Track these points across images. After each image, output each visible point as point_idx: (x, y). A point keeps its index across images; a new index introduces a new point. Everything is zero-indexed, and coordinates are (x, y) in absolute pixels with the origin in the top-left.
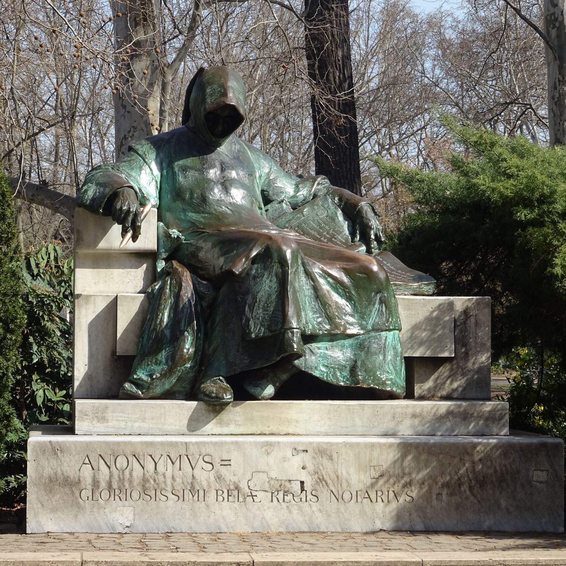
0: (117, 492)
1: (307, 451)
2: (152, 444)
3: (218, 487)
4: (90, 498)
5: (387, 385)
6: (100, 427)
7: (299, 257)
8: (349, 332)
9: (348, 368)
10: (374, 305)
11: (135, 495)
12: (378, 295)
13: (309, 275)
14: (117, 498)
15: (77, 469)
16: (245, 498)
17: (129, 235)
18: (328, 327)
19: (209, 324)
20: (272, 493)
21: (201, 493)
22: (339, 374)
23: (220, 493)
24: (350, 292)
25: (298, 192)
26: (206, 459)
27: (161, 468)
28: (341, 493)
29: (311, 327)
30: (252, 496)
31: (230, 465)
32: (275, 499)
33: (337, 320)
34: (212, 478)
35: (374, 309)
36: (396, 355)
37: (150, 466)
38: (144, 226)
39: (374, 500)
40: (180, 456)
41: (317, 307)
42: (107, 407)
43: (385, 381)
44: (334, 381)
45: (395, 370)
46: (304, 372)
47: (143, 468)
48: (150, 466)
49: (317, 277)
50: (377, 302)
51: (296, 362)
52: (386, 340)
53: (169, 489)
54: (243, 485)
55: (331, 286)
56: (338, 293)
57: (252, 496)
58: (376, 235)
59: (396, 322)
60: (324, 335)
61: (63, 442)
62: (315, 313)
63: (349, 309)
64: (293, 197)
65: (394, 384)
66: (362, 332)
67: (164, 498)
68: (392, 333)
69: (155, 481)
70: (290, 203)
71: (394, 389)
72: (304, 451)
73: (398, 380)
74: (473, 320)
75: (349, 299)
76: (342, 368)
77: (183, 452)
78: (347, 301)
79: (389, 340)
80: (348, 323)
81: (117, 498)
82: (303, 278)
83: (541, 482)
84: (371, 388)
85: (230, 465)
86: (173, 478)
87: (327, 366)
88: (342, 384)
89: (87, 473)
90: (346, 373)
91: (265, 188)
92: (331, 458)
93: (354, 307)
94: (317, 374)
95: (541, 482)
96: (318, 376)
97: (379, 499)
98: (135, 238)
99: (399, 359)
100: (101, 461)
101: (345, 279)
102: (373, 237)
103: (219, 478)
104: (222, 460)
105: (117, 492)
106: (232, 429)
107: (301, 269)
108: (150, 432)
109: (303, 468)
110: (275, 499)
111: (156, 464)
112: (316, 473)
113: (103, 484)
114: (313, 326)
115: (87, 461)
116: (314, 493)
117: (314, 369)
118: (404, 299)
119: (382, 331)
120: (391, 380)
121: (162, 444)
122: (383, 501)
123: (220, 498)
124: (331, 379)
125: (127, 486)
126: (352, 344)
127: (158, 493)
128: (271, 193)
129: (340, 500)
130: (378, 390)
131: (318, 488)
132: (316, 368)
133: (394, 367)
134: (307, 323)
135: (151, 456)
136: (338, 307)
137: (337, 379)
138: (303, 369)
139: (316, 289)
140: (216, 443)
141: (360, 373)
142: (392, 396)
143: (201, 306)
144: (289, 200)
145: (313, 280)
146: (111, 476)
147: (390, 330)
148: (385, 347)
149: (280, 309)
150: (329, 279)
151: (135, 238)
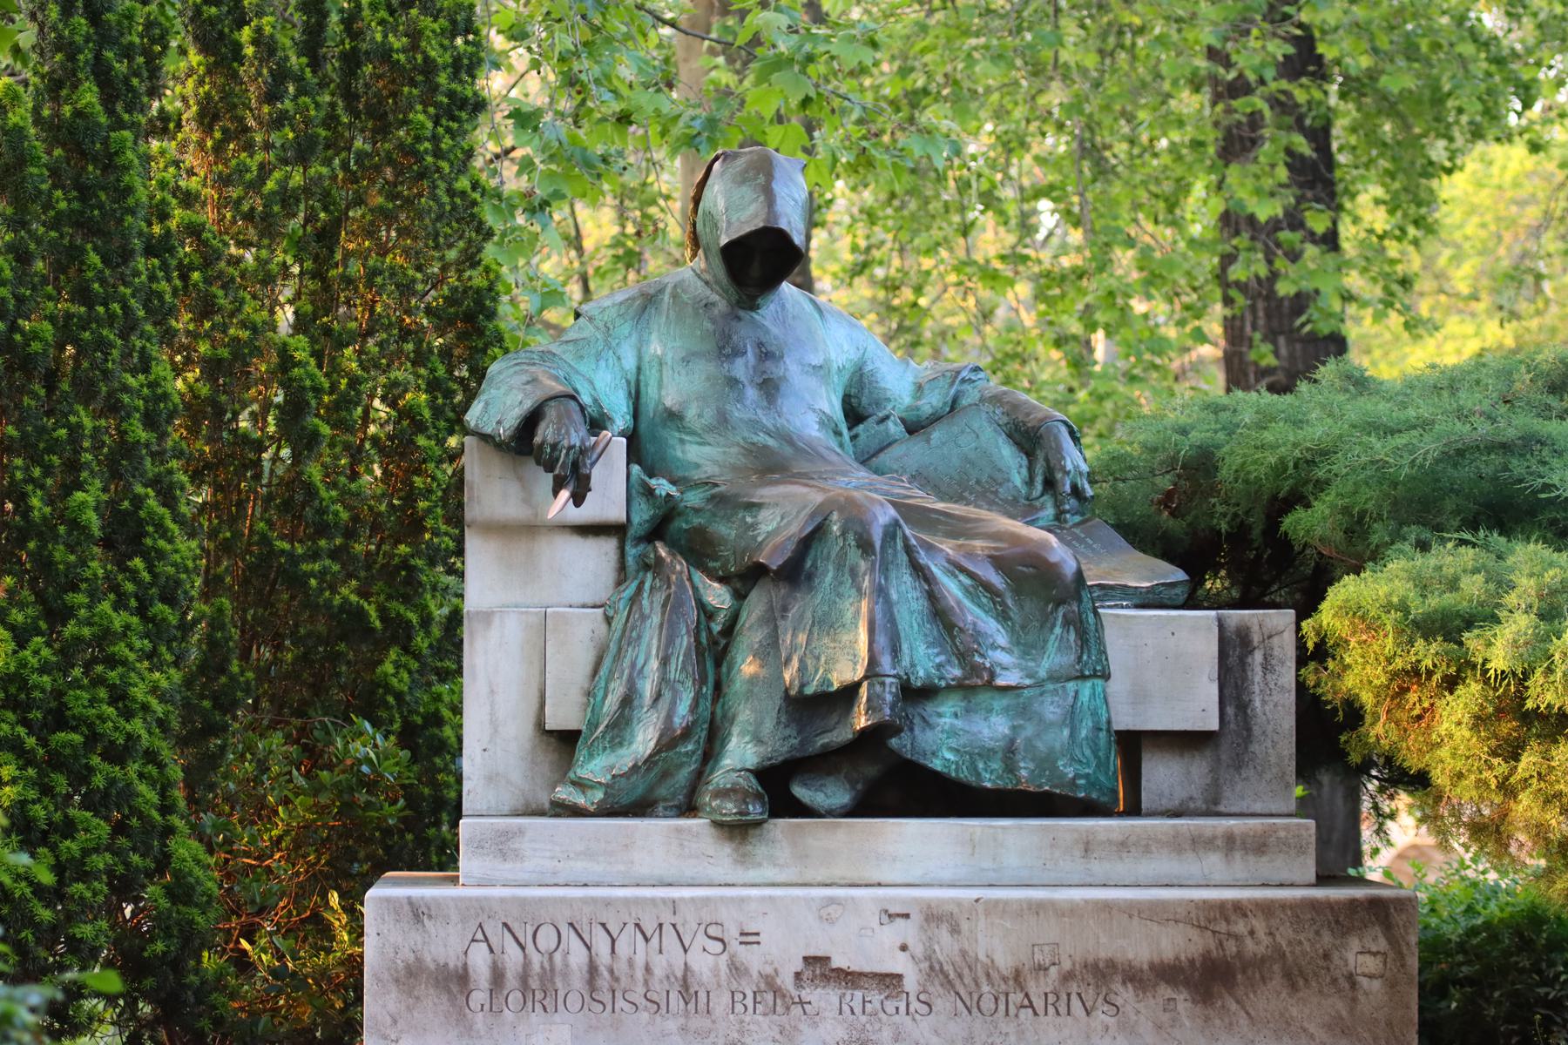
0: (539, 995)
1: (907, 916)
2: (608, 903)
3: (734, 986)
4: (487, 1007)
6: (506, 869)
7: (899, 533)
8: (1000, 682)
9: (1000, 755)
10: (1053, 626)
11: (574, 1001)
13: (919, 571)
14: (538, 1005)
15: (460, 950)
16: (788, 1008)
17: (565, 494)
19: (724, 669)
22: (981, 766)
23: (739, 997)
24: (1003, 604)
25: (919, 399)
26: (712, 931)
27: (623, 947)
28: (975, 997)
29: (921, 673)
33: (977, 658)
34: (724, 968)
37: (601, 944)
38: (597, 474)
39: (1041, 1011)
40: (661, 925)
42: (521, 832)
43: (1074, 779)
44: (972, 779)
45: (1096, 757)
47: (589, 948)
48: (601, 944)
50: (1059, 622)
51: (894, 742)
53: (641, 990)
55: (966, 590)
56: (980, 606)
58: (1075, 488)
59: (1099, 661)
60: (949, 687)
61: (434, 899)
63: (1002, 639)
64: (909, 408)
65: (1092, 784)
66: (1028, 682)
67: (627, 1007)
68: (1089, 684)
69: (611, 972)
70: (903, 420)
71: (1094, 796)
73: (1102, 778)
74: (1258, 657)
75: (1003, 617)
76: (987, 754)
77: (667, 918)
81: (538, 1005)
82: (907, 578)
83: (1371, 977)
86: (648, 969)
87: (958, 751)
88: (988, 785)
89: (479, 960)
90: (996, 765)
91: (853, 391)
92: (955, 930)
93: (1012, 631)
94: (937, 765)
95: (1371, 977)
96: (939, 769)
97: (1051, 1010)
98: (578, 499)
99: (1103, 735)
100: (507, 935)
101: (997, 580)
102: (1068, 488)
103: (737, 969)
105: (539, 995)
106: (769, 873)
107: (903, 558)
108: (608, 880)
109: (904, 948)
111: (613, 941)
112: (928, 958)
113: (511, 980)
115: (479, 936)
116: (922, 997)
118: (1118, 616)
119: (1069, 679)
120: (1087, 776)
121: (626, 901)
122: (1058, 1013)
123: (739, 1008)
124: (965, 775)
125: (559, 985)
127: (618, 995)
128: (864, 401)
129: (975, 1010)
130: (1060, 796)
131: (931, 989)
132: (933, 754)
134: (913, 665)
135: (603, 925)
136: (978, 634)
137: (978, 774)
140: (732, 899)
143: (709, 630)
144: (904, 415)
145: (927, 580)
146: (527, 964)
147: (1083, 677)
150: (962, 577)
151: (578, 499)
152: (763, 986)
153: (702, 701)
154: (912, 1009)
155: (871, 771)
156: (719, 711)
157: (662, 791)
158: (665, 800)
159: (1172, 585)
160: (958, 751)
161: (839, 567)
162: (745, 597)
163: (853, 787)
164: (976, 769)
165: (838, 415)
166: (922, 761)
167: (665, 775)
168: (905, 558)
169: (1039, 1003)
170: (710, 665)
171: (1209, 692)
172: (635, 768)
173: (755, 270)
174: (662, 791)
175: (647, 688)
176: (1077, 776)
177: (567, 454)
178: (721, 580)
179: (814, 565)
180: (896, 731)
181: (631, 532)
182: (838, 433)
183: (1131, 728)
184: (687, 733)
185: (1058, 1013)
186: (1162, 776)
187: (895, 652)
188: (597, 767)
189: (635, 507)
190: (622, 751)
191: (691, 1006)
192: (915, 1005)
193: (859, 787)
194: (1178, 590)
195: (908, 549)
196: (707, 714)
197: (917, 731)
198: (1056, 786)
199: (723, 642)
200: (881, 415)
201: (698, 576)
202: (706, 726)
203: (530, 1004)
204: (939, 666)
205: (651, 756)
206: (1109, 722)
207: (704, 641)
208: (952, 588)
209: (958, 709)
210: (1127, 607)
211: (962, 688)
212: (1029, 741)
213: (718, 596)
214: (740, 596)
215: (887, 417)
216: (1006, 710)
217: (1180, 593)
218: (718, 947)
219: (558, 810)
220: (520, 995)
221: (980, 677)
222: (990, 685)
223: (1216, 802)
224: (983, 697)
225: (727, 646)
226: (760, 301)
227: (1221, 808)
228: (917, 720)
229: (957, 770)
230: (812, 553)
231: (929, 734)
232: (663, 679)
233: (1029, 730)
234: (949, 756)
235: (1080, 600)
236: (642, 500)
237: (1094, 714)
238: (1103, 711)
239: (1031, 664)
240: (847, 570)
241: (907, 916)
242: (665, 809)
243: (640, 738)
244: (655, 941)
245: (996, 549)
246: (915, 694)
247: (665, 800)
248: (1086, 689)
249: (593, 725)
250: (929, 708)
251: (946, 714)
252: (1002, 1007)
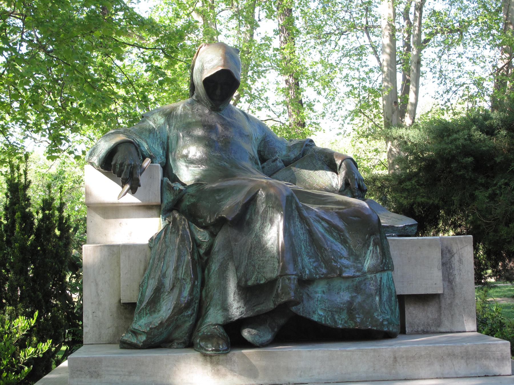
5: (384, 325)
8: (345, 275)
9: (346, 311)
10: (369, 246)
12: (372, 237)
18: (324, 271)
19: (206, 272)
22: (336, 317)
29: (307, 272)
35: (369, 251)
36: (390, 296)
41: (313, 251)
43: (382, 322)
45: (391, 310)
46: (302, 317)
49: (312, 221)
51: (294, 309)
52: (381, 281)
55: (326, 229)
62: (310, 257)
65: (389, 323)
66: (358, 274)
70: (283, 161)
71: (391, 329)
73: (393, 320)
74: (456, 257)
75: (344, 242)
76: (340, 310)
78: (342, 244)
79: (384, 281)
80: (347, 267)
82: (298, 223)
84: (370, 329)
87: (325, 310)
88: (340, 326)
90: (344, 316)
91: (262, 149)
94: (315, 318)
96: (316, 320)
99: (393, 298)
107: (296, 213)
114: (310, 271)
118: (394, 240)
119: (377, 272)
120: (387, 320)
124: (329, 322)
126: (349, 286)
133: (389, 307)
134: (303, 268)
137: (336, 322)
138: (301, 314)
139: (311, 233)
141: (357, 316)
142: (388, 336)
143: (199, 252)
144: (283, 159)
147: (383, 270)
148: (380, 288)
150: (323, 223)
153: (195, 289)
155: (282, 321)
156: (204, 293)
157: (176, 335)
158: (177, 339)
159: (411, 226)
160: (325, 310)
162: (216, 235)
163: (273, 330)
164: (334, 319)
165: (257, 156)
166: (308, 317)
167: (177, 327)
168: (297, 213)
170: (199, 270)
171: (437, 274)
172: (161, 324)
173: (218, 92)
174: (176, 335)
175: (168, 283)
176: (384, 320)
177: (127, 168)
178: (205, 228)
179: (251, 218)
180: (297, 303)
181: (163, 207)
182: (257, 163)
183: (402, 293)
184: (188, 305)
186: (414, 314)
187: (295, 262)
188: (143, 323)
189: (165, 196)
190: (155, 315)
193: (276, 330)
194: (413, 228)
195: (298, 208)
196: (198, 295)
197: (305, 302)
198: (374, 326)
199: (206, 258)
200: (274, 158)
201: (193, 226)
202: (197, 301)
204: (315, 268)
205: (169, 318)
206: (395, 292)
207: (196, 257)
208: (319, 229)
209: (324, 289)
210: (395, 236)
211: (326, 278)
212: (360, 304)
213: (202, 236)
214: (213, 235)
215: (276, 159)
216: (348, 288)
217: (414, 229)
219: (125, 346)
221: (335, 272)
222: (340, 276)
223: (439, 326)
224: (337, 283)
225: (207, 262)
226: (221, 107)
227: (442, 330)
228: (305, 296)
229: (325, 320)
230: (249, 211)
231: (311, 302)
232: (176, 279)
233: (360, 299)
234: (321, 313)
235: (380, 233)
236: (168, 192)
237: (389, 288)
238: (392, 287)
239: (360, 265)
242: (178, 344)
243: (164, 308)
245: (339, 209)
246: (304, 283)
247: (177, 339)
248: (385, 275)
249: (141, 302)
250: (311, 288)
251: (319, 290)
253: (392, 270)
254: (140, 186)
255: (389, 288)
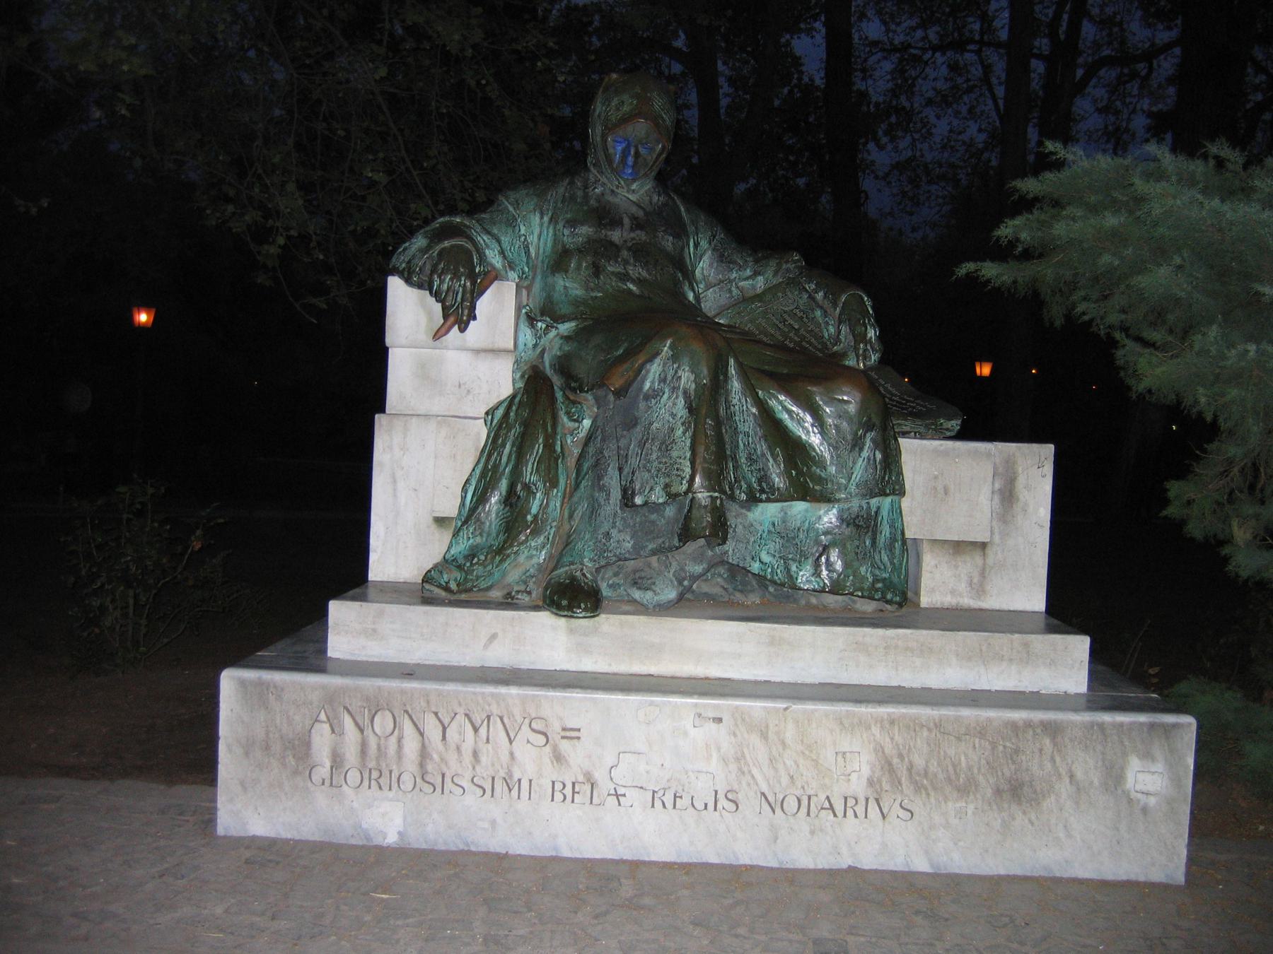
0: (375, 774)
4: (327, 782)
10: (861, 449)
14: (373, 783)
20: (654, 792)
21: (525, 784)
23: (558, 786)
30: (617, 795)
31: (578, 738)
32: (658, 804)
36: (893, 539)
37: (433, 731)
39: (840, 813)
40: (489, 717)
47: (422, 734)
48: (433, 731)
54: (600, 775)
57: (617, 795)
68: (889, 499)
72: (714, 719)
77: (495, 710)
79: (885, 512)
85: (578, 738)
97: (850, 813)
104: (564, 729)
105: (375, 774)
110: (658, 804)
111: (444, 729)
116: (730, 796)
117: (748, 559)
122: (856, 816)
123: (559, 796)
129: (778, 810)
135: (436, 714)
147: (883, 494)
149: (688, 455)
152: (581, 778)
154: (719, 806)
161: (674, 389)
169: (839, 808)
185: (856, 816)
191: (515, 792)
192: (722, 802)
203: (366, 783)
206: (903, 533)
218: (542, 739)
220: (358, 774)
240: (680, 394)
241: (720, 720)
244: (483, 731)
252: (804, 810)
253: (902, 493)
254: (475, 318)
255: (892, 526)
